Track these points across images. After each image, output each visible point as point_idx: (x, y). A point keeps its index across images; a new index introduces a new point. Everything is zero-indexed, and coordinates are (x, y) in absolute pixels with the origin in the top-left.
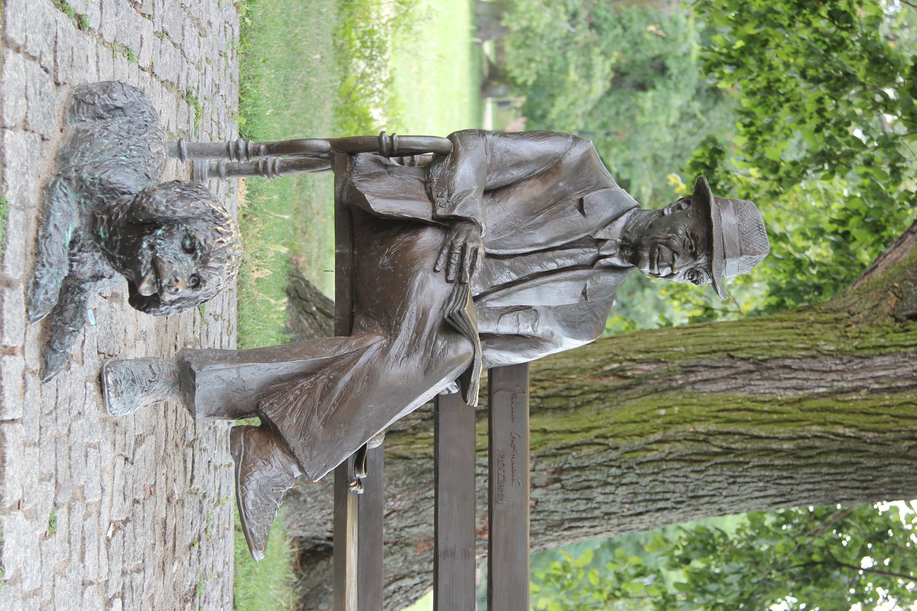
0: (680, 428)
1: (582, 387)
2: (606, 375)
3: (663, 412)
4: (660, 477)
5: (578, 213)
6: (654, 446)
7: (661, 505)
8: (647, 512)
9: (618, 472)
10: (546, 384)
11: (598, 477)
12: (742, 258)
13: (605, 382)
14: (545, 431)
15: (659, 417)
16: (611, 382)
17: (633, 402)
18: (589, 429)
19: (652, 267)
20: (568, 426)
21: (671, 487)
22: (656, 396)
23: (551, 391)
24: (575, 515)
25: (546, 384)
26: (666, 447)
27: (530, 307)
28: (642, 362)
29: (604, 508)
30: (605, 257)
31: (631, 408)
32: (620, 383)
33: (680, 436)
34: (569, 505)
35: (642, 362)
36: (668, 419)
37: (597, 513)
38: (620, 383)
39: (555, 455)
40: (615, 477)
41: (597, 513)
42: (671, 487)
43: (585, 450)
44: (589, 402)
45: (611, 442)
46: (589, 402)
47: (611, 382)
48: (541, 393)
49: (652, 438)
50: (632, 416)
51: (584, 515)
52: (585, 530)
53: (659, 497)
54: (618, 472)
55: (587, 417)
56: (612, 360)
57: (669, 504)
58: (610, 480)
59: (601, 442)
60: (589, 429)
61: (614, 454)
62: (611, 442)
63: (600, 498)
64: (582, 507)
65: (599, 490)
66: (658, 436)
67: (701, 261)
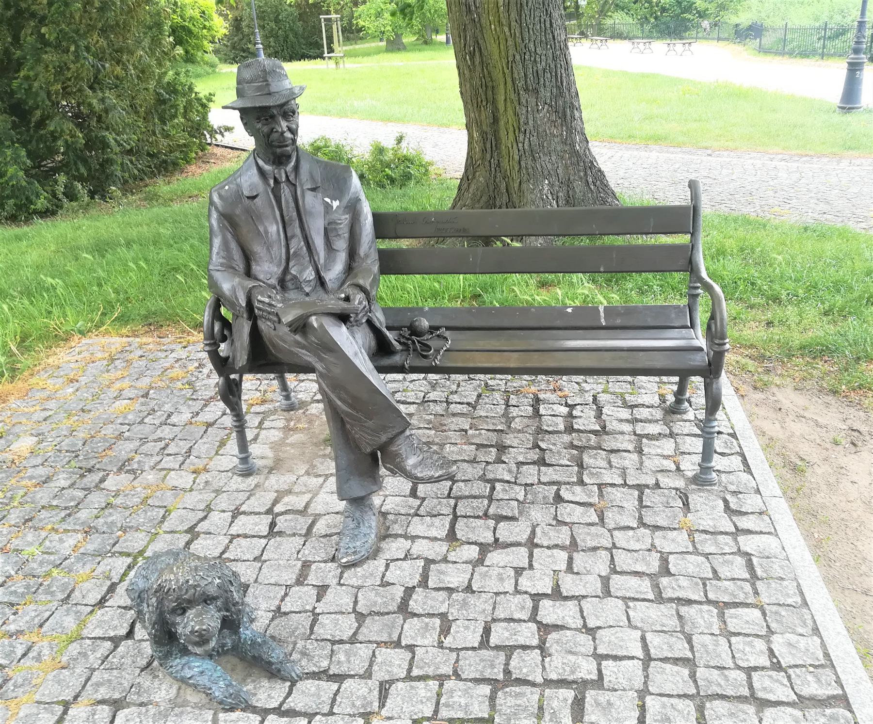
0: (501, 16)
1: (481, 79)
2: (473, 63)
3: (493, 27)
4: (531, 27)
5: (256, 200)
6: (513, 31)
7: (548, 25)
8: (552, 32)
9: (528, 53)
10: (479, 99)
11: (530, 67)
12: (270, 80)
13: (477, 63)
14: (505, 100)
15: (495, 29)
16: (477, 60)
17: (488, 45)
18: (504, 73)
19: (287, 146)
20: (502, 86)
21: (537, 19)
22: (485, 31)
23: (483, 97)
24: (554, 80)
25: (479, 99)
26: (513, 24)
27: (325, 229)
28: (465, 39)
29: (549, 61)
30: (287, 177)
31: (492, 48)
32: (477, 54)
33: (506, 15)
34: (547, 83)
35: (465, 39)
36: (497, 24)
37: (552, 66)
38: (477, 54)
39: (519, 94)
40: (531, 56)
41: (552, 66)
42: (537, 19)
43: (516, 75)
44: (489, 73)
45: (510, 59)
46: (489, 73)
47: (477, 60)
48: (484, 103)
49: (508, 34)
50: (495, 46)
51: (554, 74)
52: (563, 71)
53: (543, 26)
54: (528, 53)
55: (498, 76)
56: (465, 59)
57: (548, 19)
58: (533, 59)
59: (510, 64)
60: (504, 73)
61: (518, 57)
62: (510, 59)
63: (544, 63)
64: (549, 75)
65: (539, 65)
66: (506, 29)
67: (275, 112)
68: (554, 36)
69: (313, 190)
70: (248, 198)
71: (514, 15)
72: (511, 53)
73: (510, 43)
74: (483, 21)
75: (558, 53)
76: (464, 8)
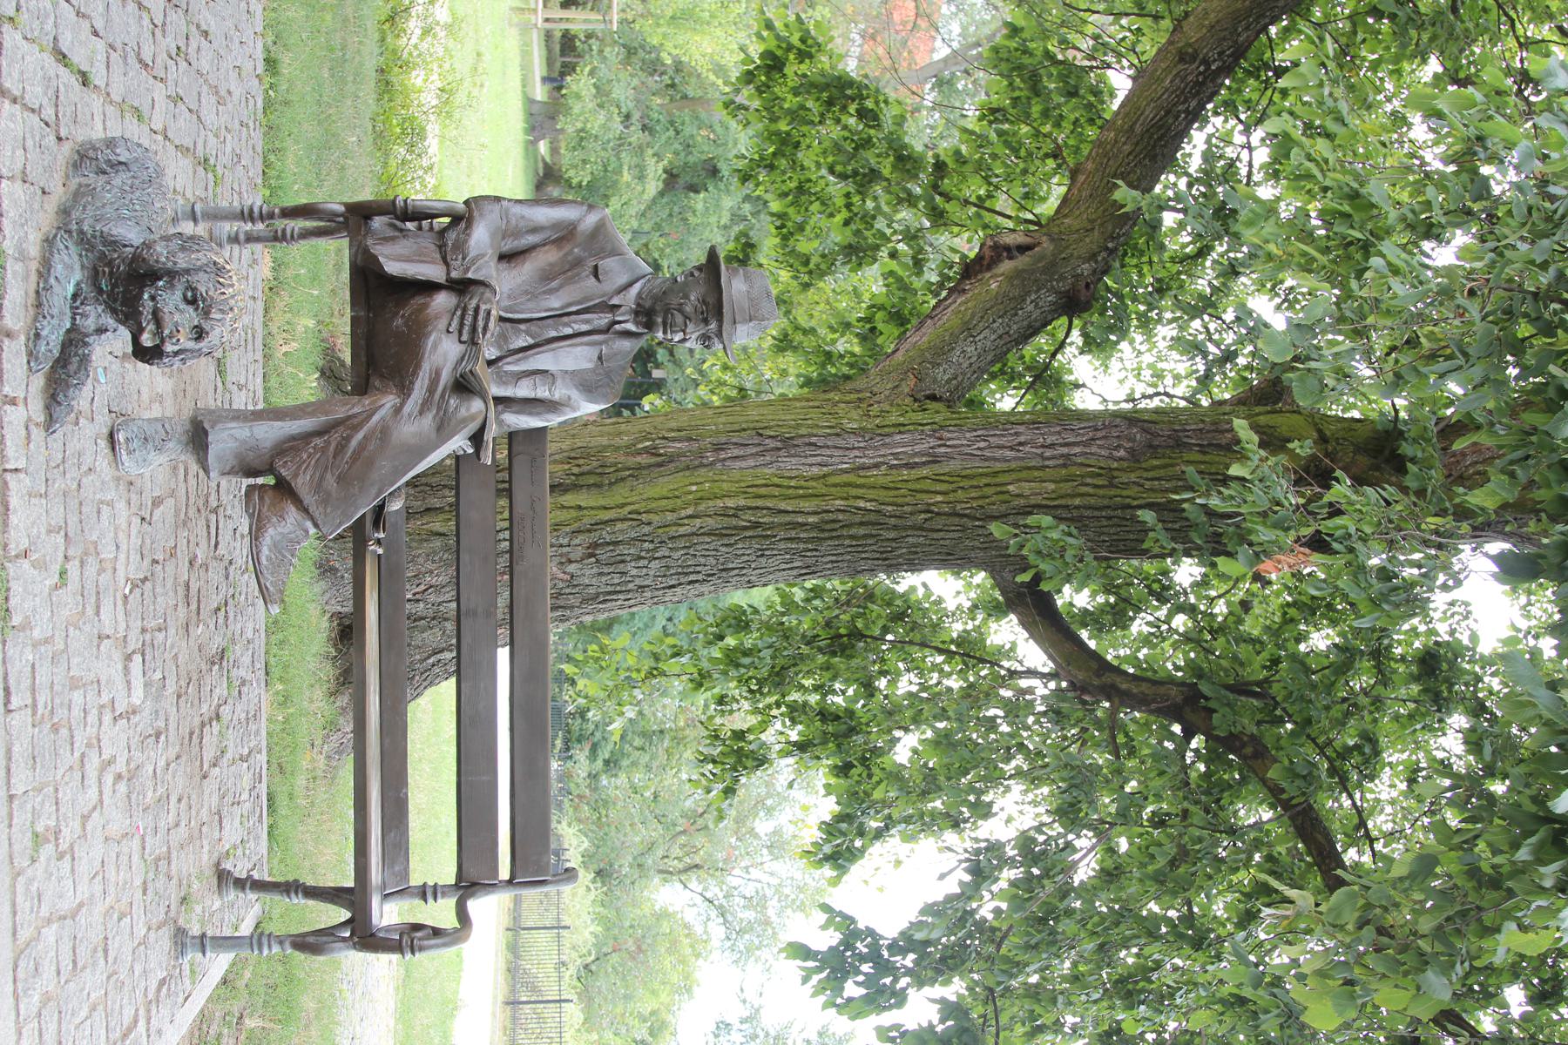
0: (711, 503)
3: (694, 488)
4: (691, 551)
5: (593, 280)
7: (692, 577)
9: (651, 546)
10: (581, 462)
11: (632, 551)
14: (580, 508)
16: (644, 459)
18: (623, 506)
19: (665, 332)
20: (602, 502)
21: (702, 560)
22: (687, 473)
23: (586, 468)
24: (609, 589)
25: (581, 462)
26: (698, 522)
28: (674, 440)
29: (638, 582)
31: (663, 485)
32: (653, 460)
33: (711, 511)
34: (604, 579)
35: (674, 440)
37: (631, 586)
38: (653, 460)
39: (589, 531)
40: (648, 551)
41: (631, 586)
42: (702, 560)
43: (619, 526)
44: (623, 479)
45: (644, 517)
46: (623, 479)
47: (644, 459)
48: (576, 470)
49: (683, 513)
50: (665, 492)
54: (651, 546)
55: (620, 494)
56: (645, 439)
57: (700, 577)
59: (635, 517)
60: (623, 506)
61: (647, 529)
62: (644, 517)
63: (634, 572)
66: (689, 511)
68: (673, 586)
69: (600, 358)
70: (596, 267)
71: (711, 523)
72: (655, 518)
73: (670, 517)
74: (703, 471)
75: (648, 594)
76: (723, 440)
